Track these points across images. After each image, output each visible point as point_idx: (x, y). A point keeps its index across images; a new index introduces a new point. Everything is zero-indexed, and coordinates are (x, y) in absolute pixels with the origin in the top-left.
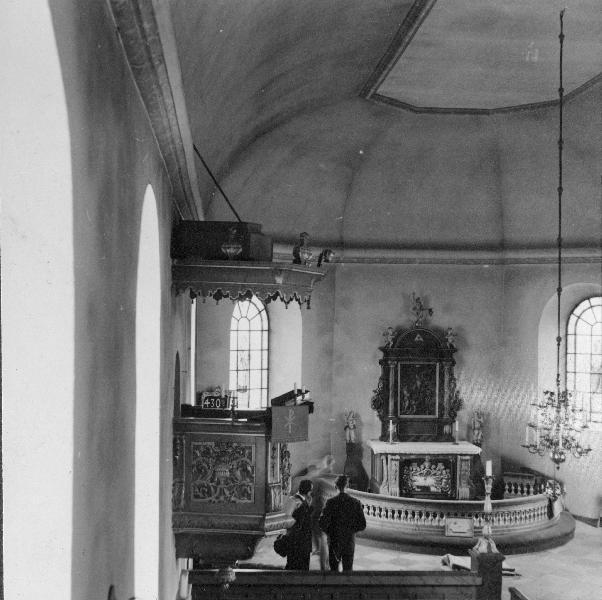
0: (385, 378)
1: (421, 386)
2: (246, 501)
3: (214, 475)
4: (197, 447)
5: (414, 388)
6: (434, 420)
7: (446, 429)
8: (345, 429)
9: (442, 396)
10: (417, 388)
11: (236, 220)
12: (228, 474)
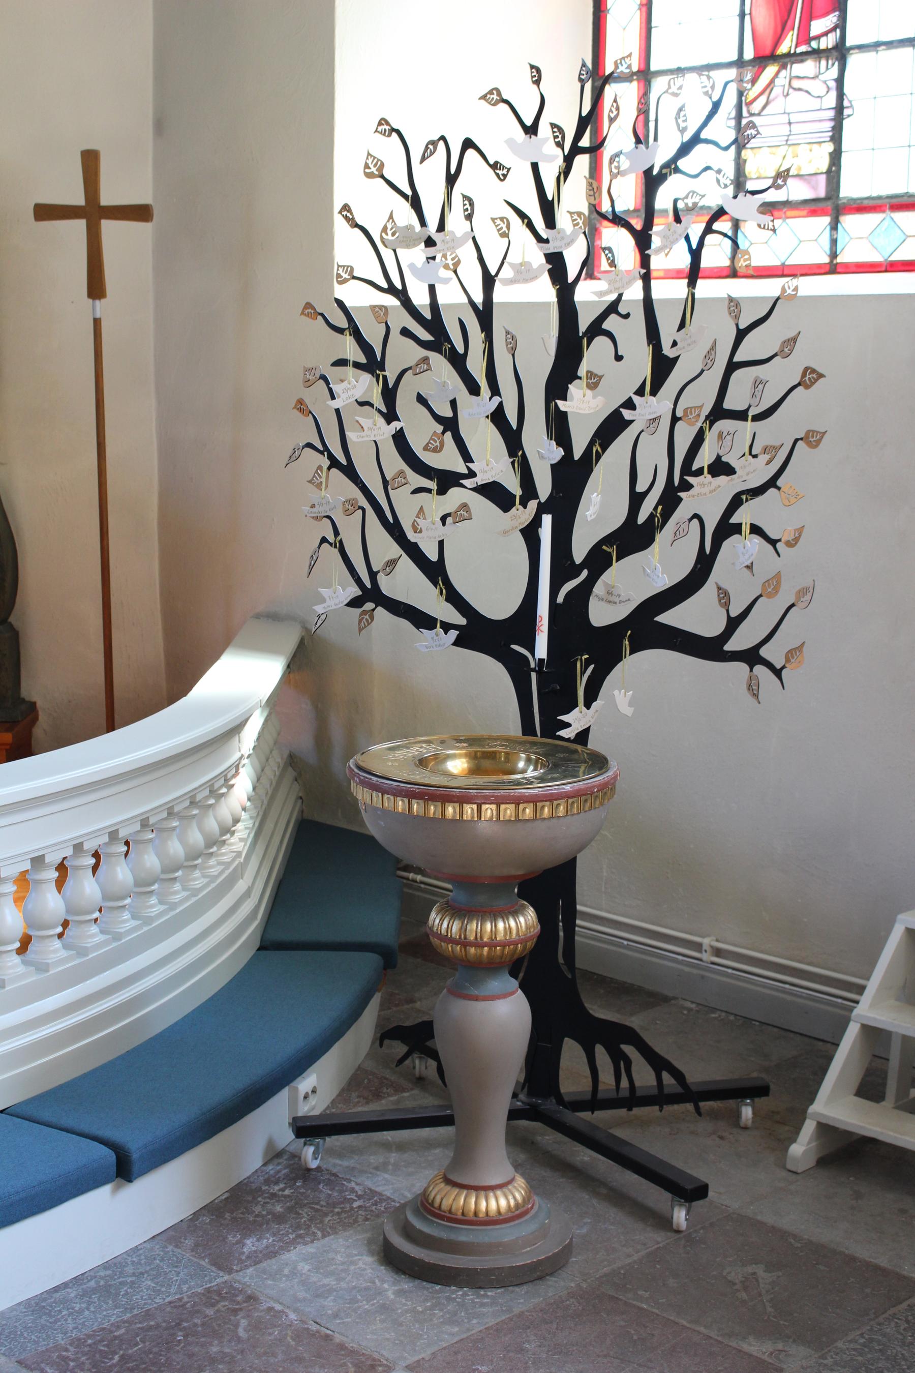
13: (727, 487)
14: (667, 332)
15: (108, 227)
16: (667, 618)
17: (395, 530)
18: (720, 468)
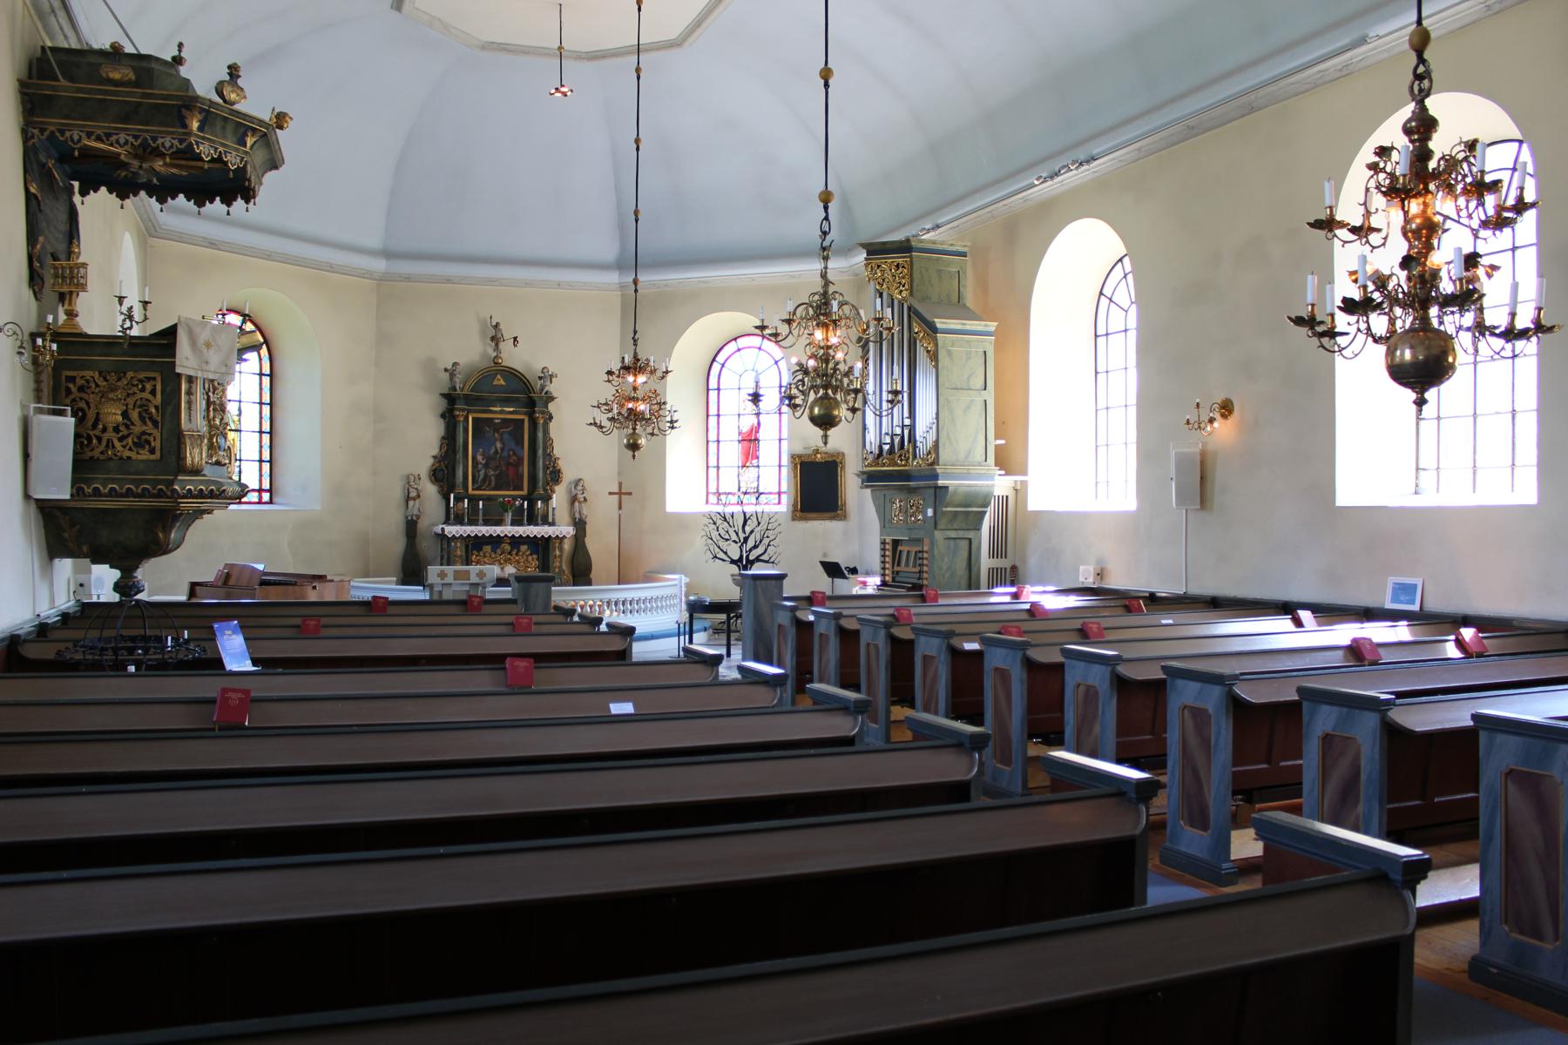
0: (450, 440)
1: (502, 449)
2: (145, 455)
3: (97, 420)
4: (72, 379)
5: (493, 451)
10: (496, 451)
11: (135, 52)
12: (120, 418)
13: (769, 540)
14: (759, 519)
15: (623, 496)
16: (762, 558)
17: (719, 547)
18: (768, 537)
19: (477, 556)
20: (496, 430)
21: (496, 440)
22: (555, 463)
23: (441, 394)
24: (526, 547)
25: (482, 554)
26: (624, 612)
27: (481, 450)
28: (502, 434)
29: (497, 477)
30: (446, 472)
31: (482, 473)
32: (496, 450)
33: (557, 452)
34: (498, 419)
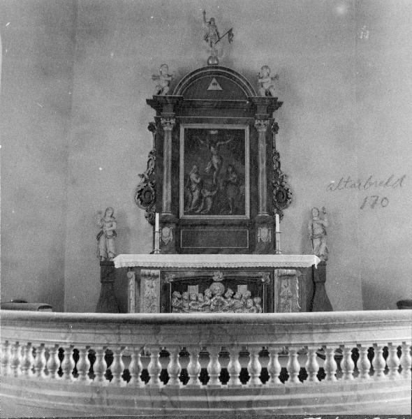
0: (158, 152)
5: (207, 169)
6: (241, 224)
7: (263, 234)
8: (98, 238)
9: (254, 182)
19: (179, 299)
20: (213, 143)
21: (212, 154)
22: (282, 181)
23: (149, 102)
24: (245, 287)
25: (185, 295)
26: (372, 372)
27: (195, 167)
28: (218, 148)
29: (213, 198)
30: (153, 193)
31: (196, 194)
32: (213, 167)
33: (285, 167)
34: (214, 130)
